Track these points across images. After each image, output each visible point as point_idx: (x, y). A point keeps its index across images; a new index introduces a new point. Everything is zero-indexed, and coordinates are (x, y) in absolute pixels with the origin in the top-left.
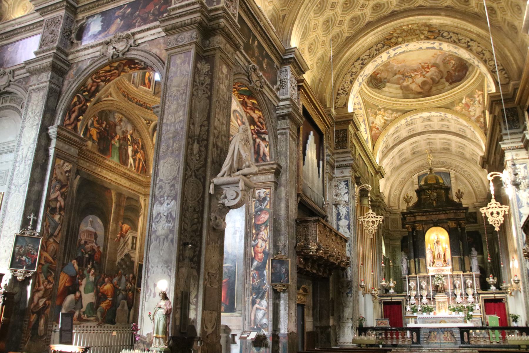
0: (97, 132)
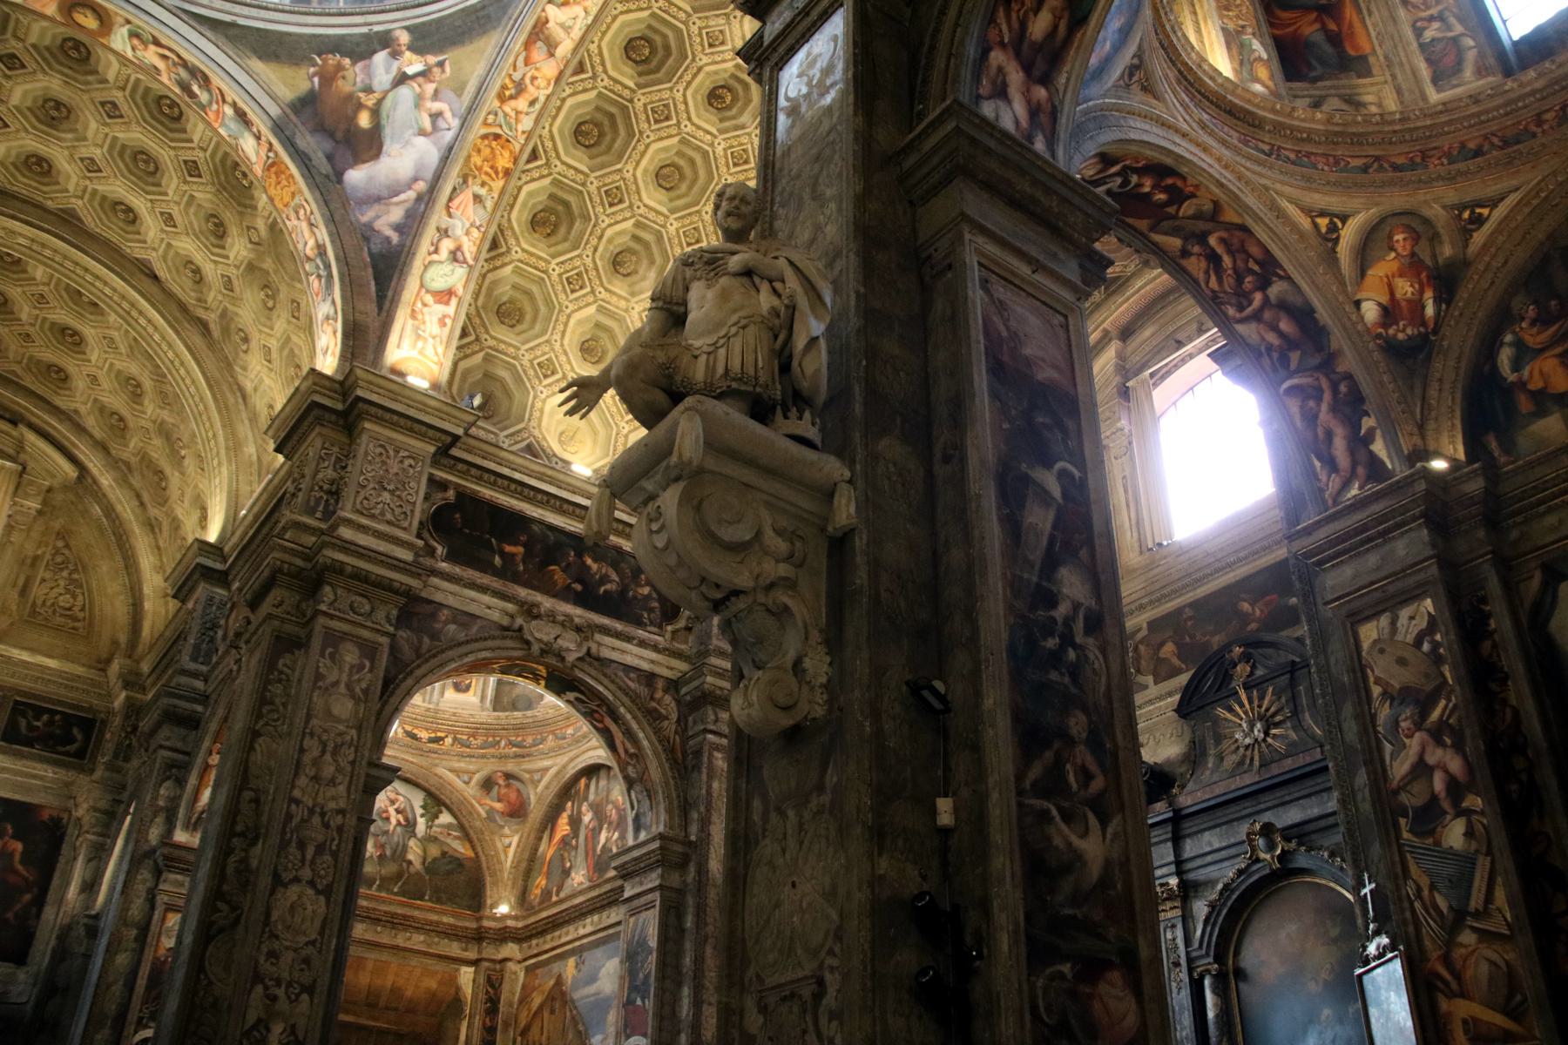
0: (1560, 356)
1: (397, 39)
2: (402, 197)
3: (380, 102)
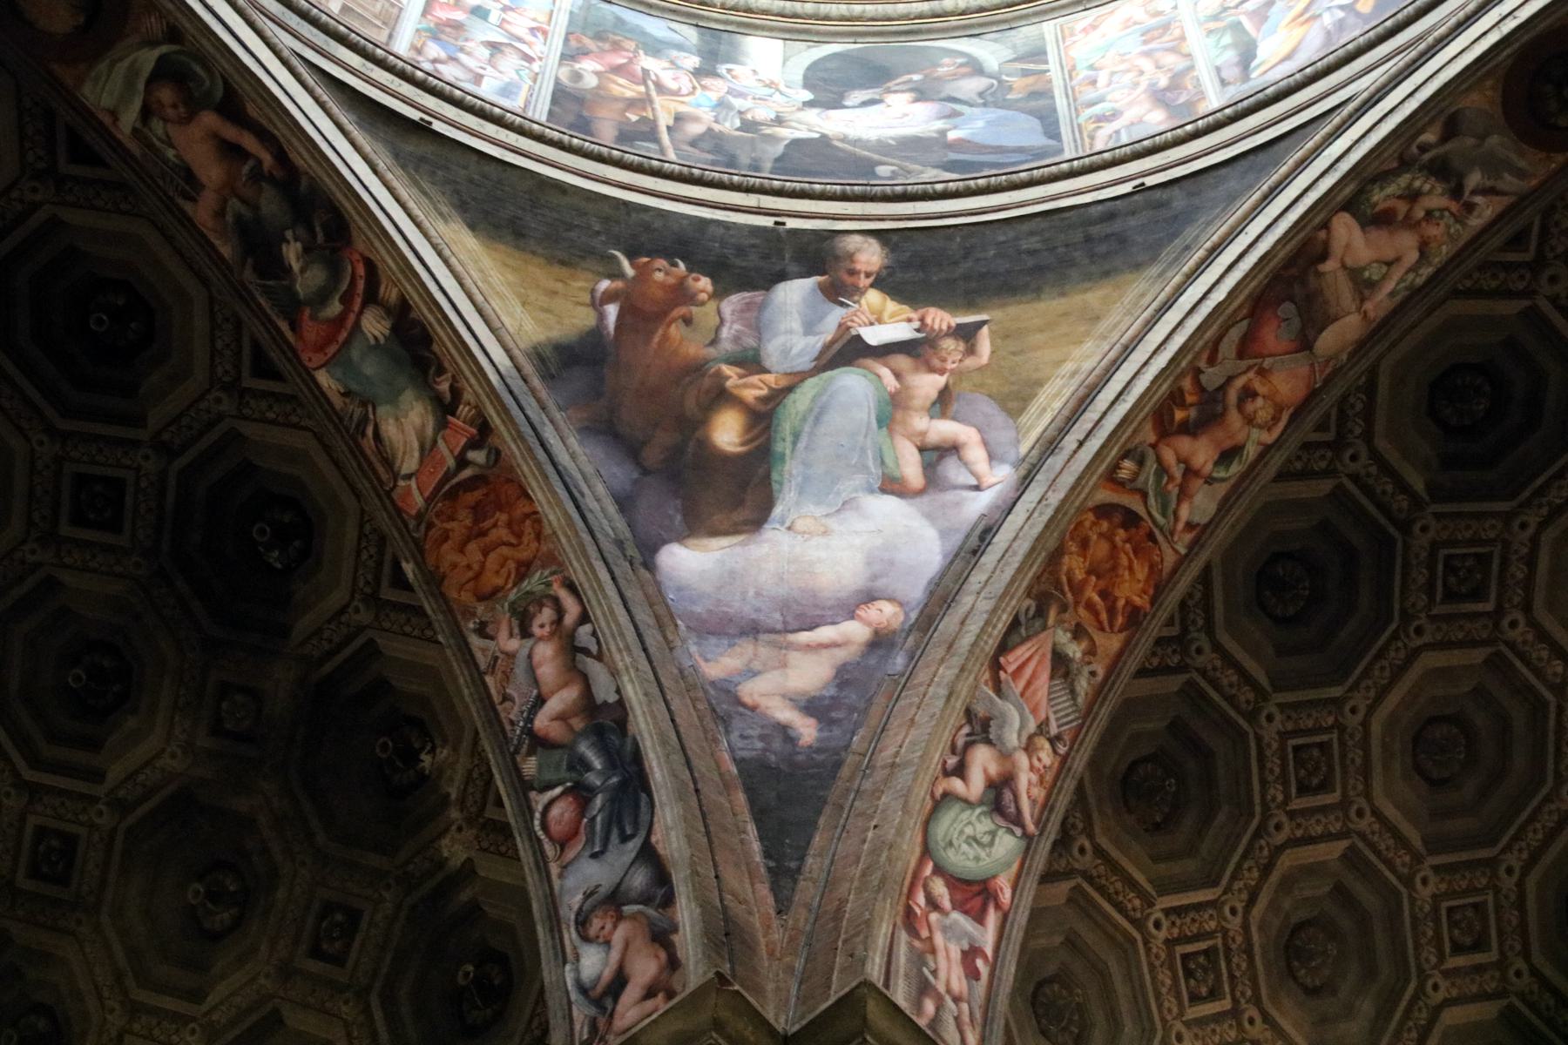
1: (851, 257)
2: (825, 633)
3: (777, 396)
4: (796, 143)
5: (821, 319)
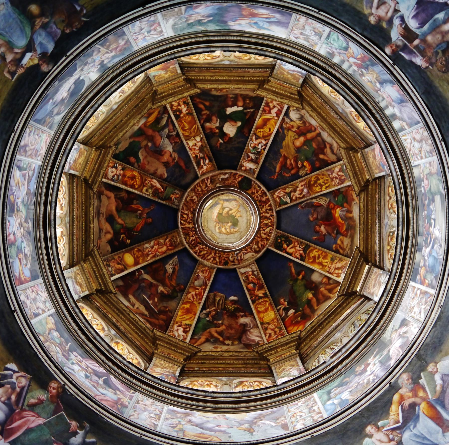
1: (48, 64)
4: (76, 70)
5: (41, 48)
